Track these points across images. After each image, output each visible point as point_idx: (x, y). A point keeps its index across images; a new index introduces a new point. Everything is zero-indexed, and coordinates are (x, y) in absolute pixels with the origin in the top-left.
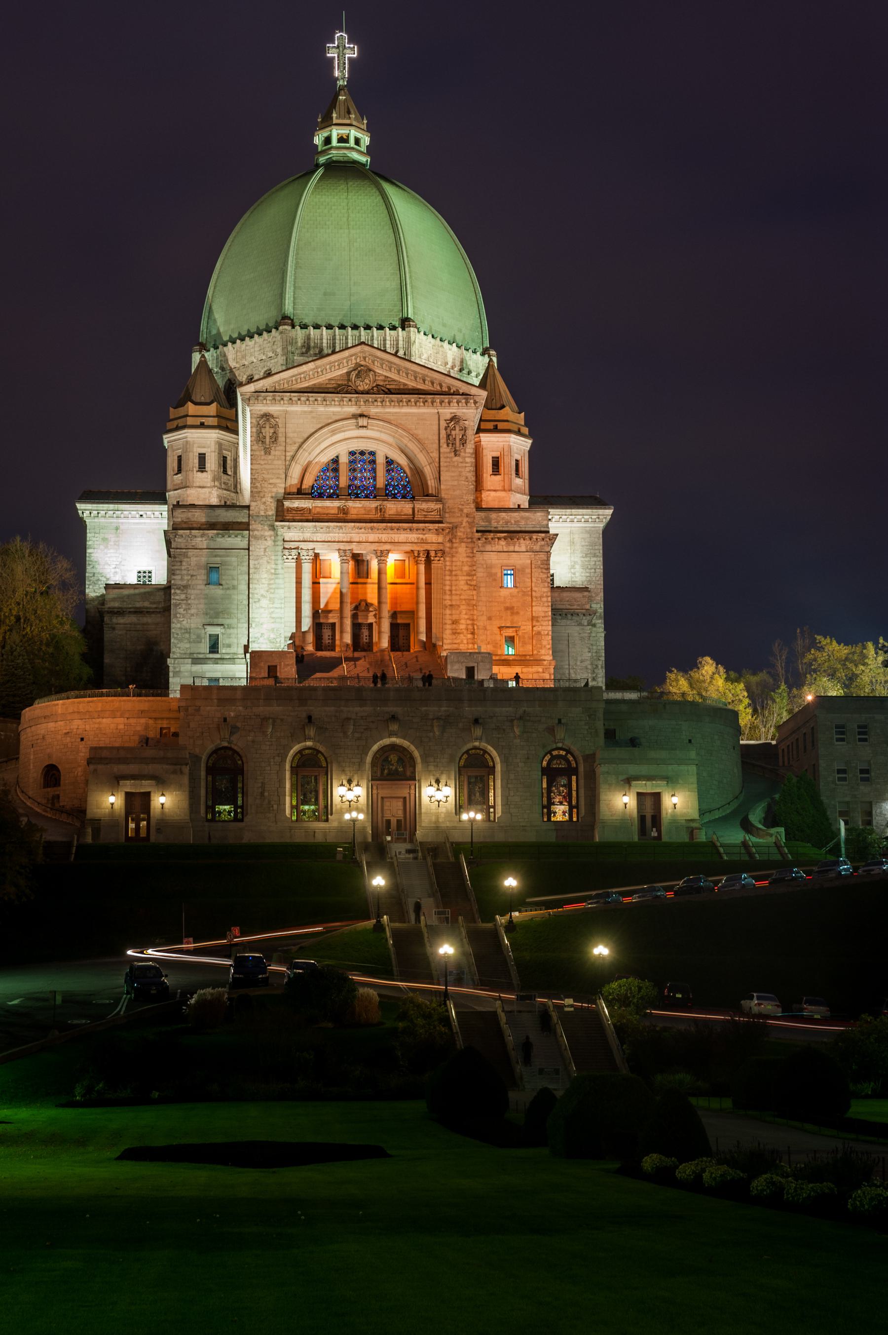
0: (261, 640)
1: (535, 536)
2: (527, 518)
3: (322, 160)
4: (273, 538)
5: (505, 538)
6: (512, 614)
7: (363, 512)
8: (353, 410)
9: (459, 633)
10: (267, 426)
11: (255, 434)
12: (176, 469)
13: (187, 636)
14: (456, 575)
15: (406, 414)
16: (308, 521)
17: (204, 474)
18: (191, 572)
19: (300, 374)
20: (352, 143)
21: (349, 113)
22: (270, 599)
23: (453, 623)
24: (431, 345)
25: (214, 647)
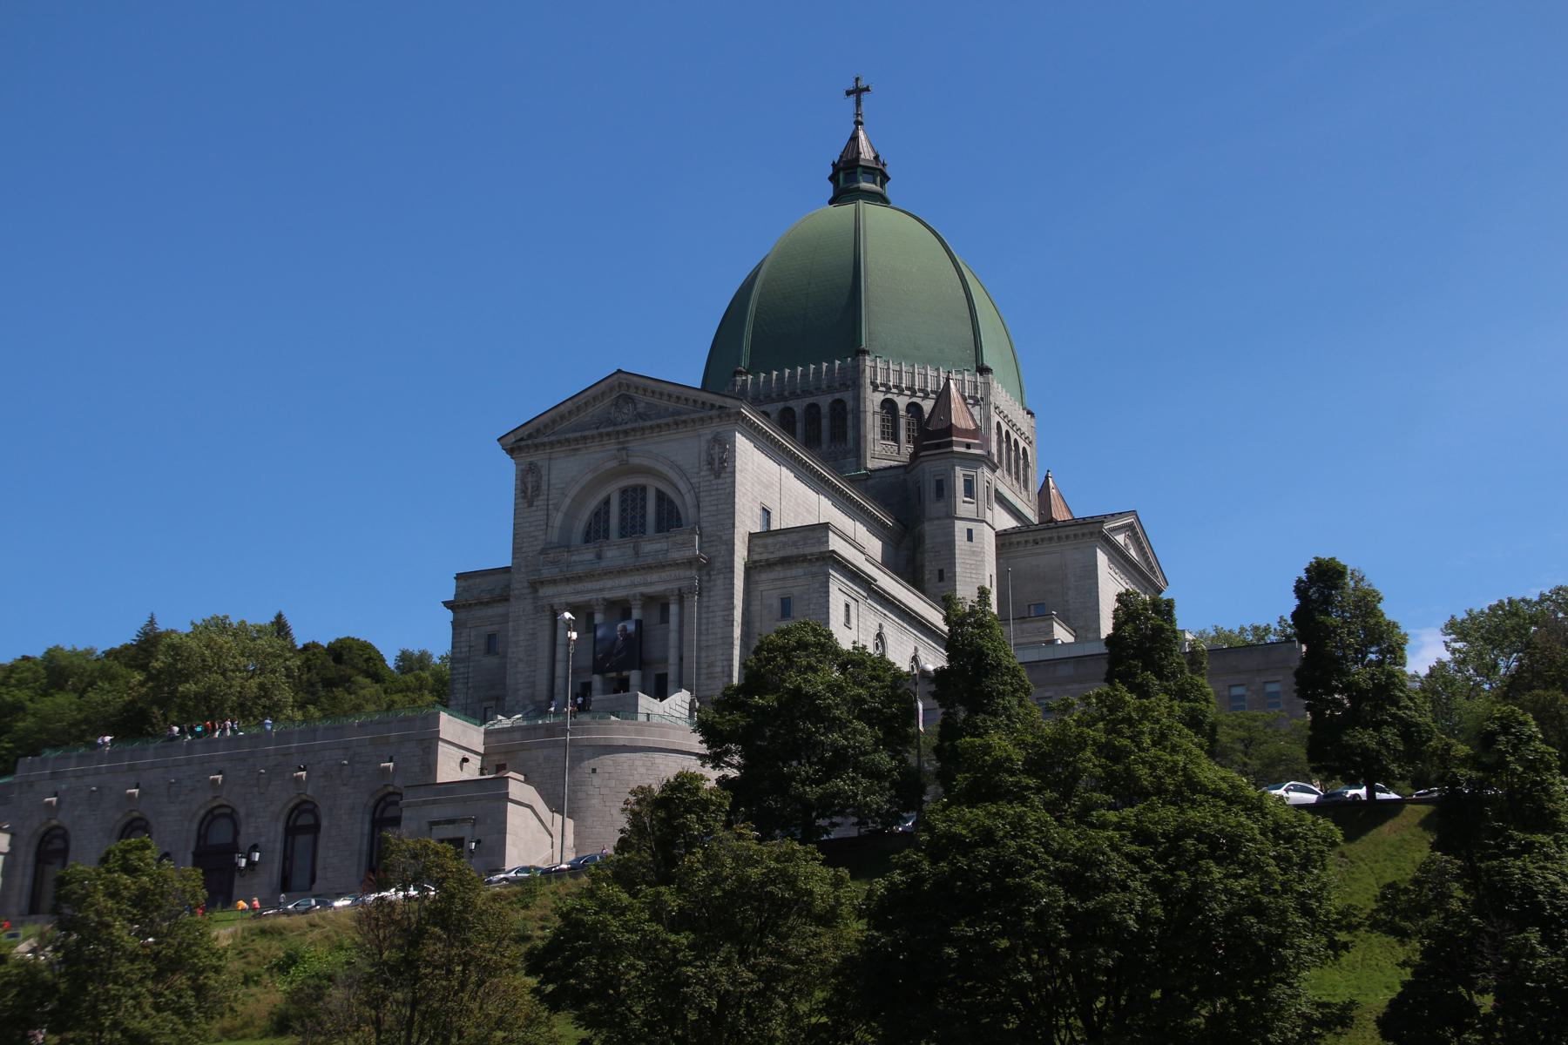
23: (708, 667)
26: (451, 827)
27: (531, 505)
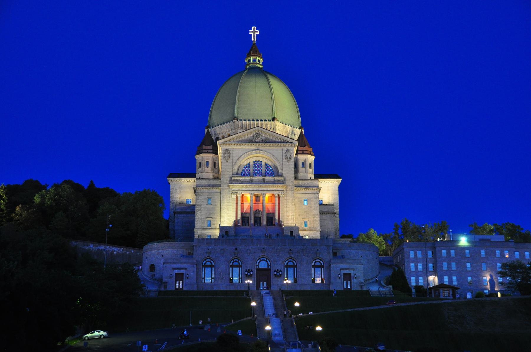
0: (224, 222)
2: (312, 183)
3: (248, 67)
4: (228, 189)
5: (304, 189)
6: (307, 214)
7: (258, 181)
8: (254, 148)
9: (289, 220)
10: (227, 153)
11: (223, 156)
12: (199, 166)
13: (200, 221)
14: (288, 201)
15: (272, 149)
16: (240, 184)
17: (208, 168)
18: (202, 201)
19: (237, 136)
21: (256, 52)
22: (227, 209)
24: (282, 126)
25: (209, 225)
26: (347, 270)
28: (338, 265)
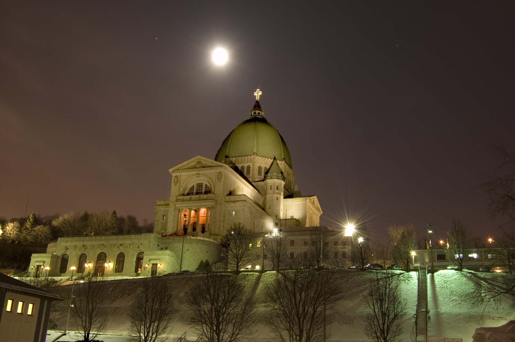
1: (240, 202)
2: (239, 197)
8: (196, 173)
20: (257, 114)
27: (176, 185)
28: (149, 256)
